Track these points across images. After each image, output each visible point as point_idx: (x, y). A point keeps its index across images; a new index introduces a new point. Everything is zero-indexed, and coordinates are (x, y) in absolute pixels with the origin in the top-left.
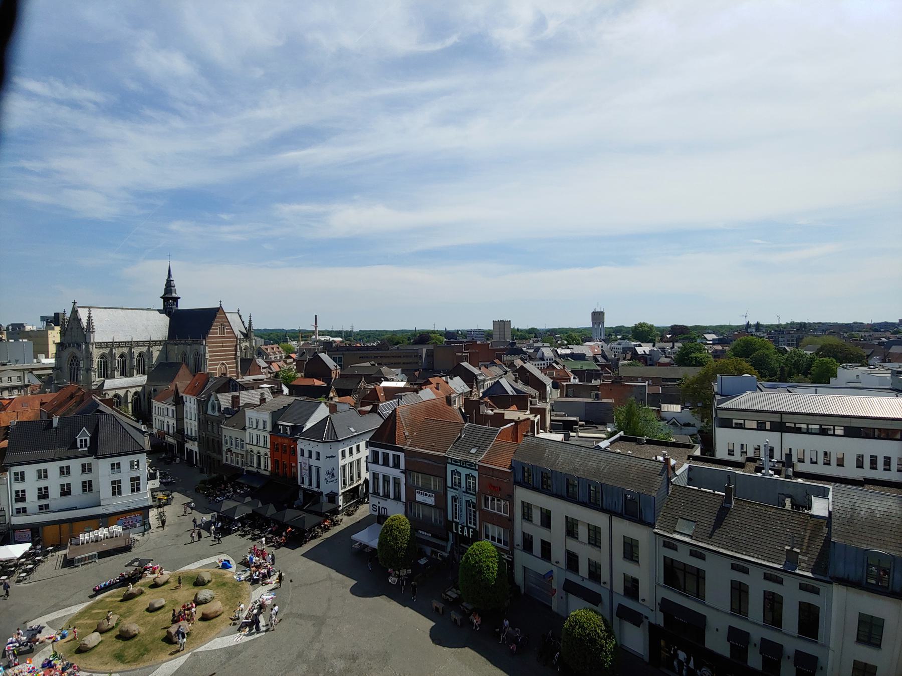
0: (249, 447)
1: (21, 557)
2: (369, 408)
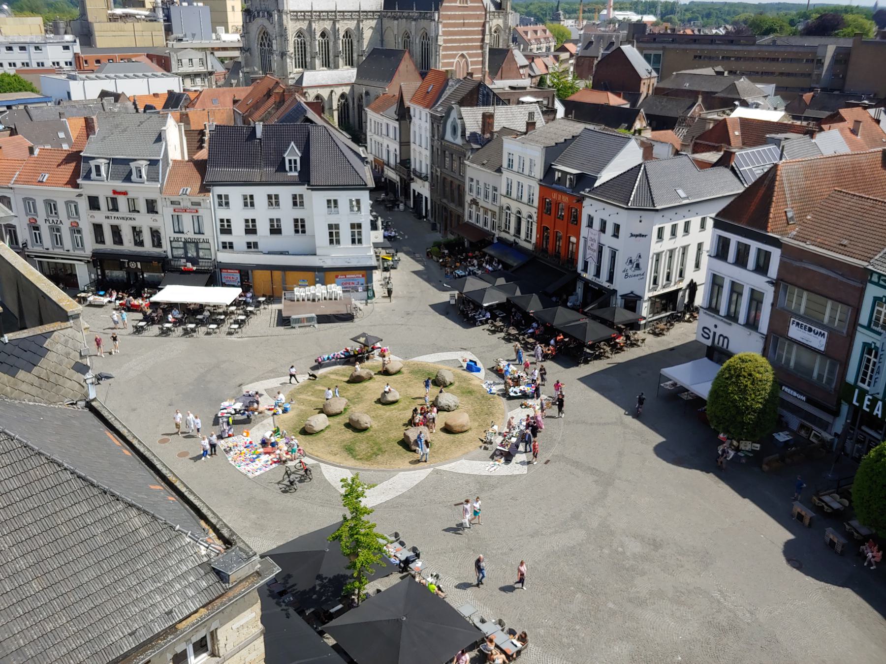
0: (505, 202)
1: (231, 305)
2: (712, 157)
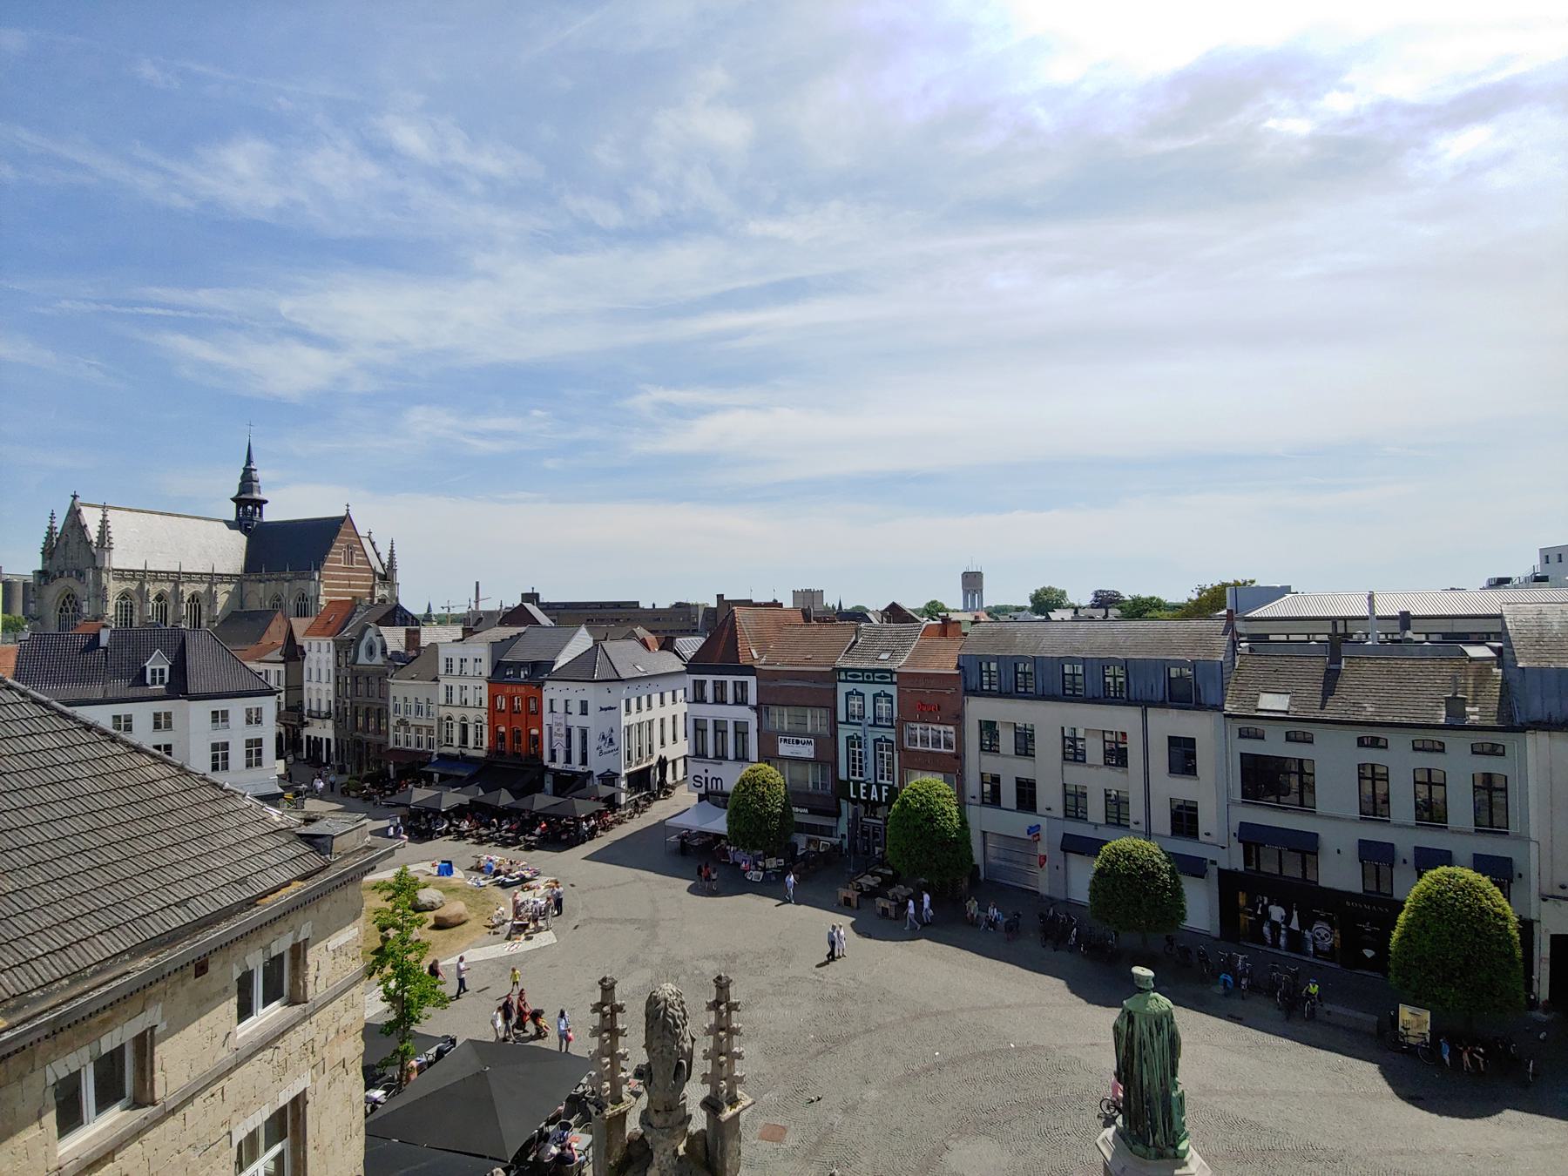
0: (444, 712)
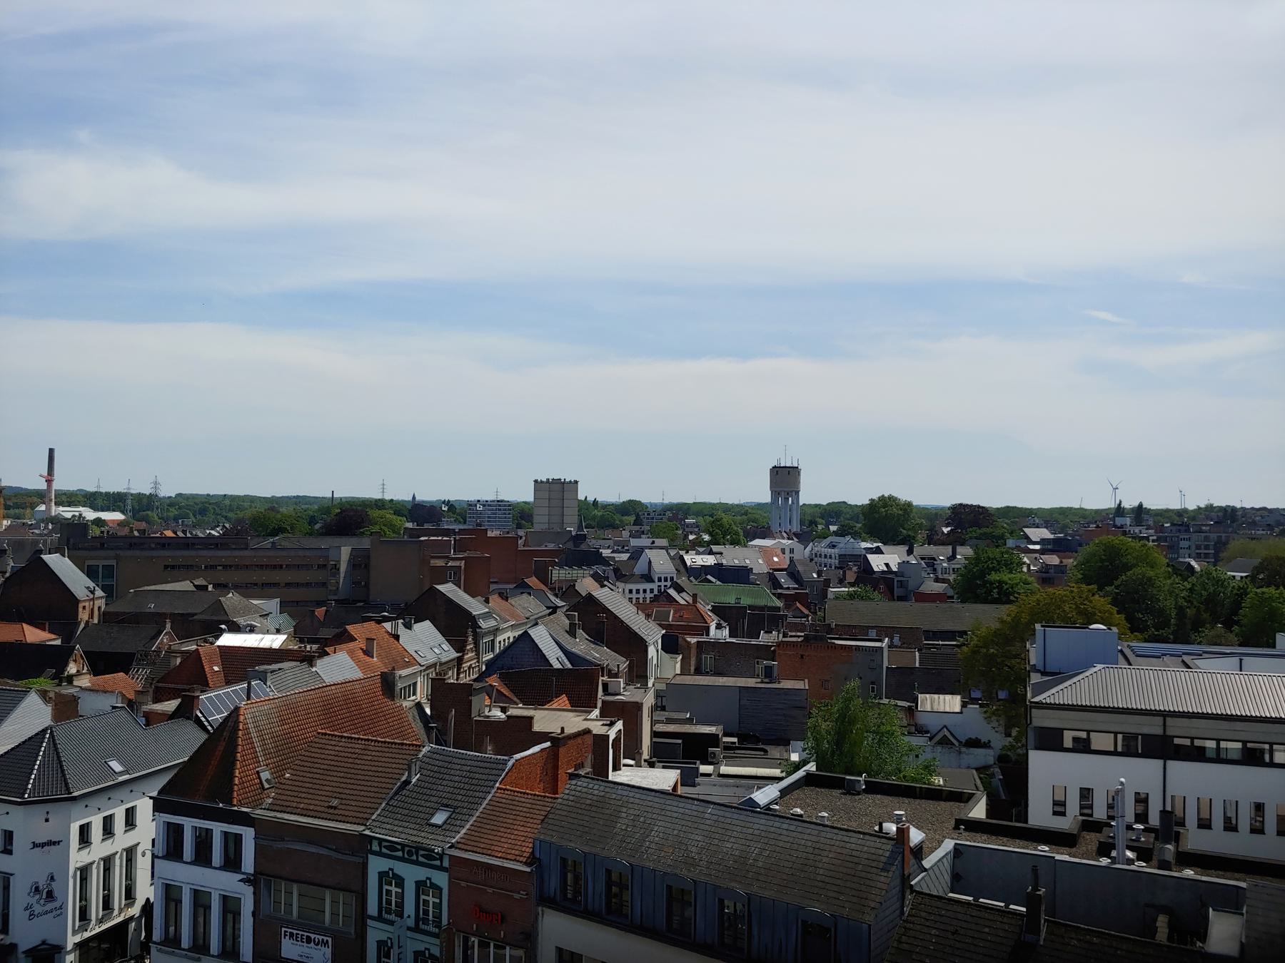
2: (171, 705)
